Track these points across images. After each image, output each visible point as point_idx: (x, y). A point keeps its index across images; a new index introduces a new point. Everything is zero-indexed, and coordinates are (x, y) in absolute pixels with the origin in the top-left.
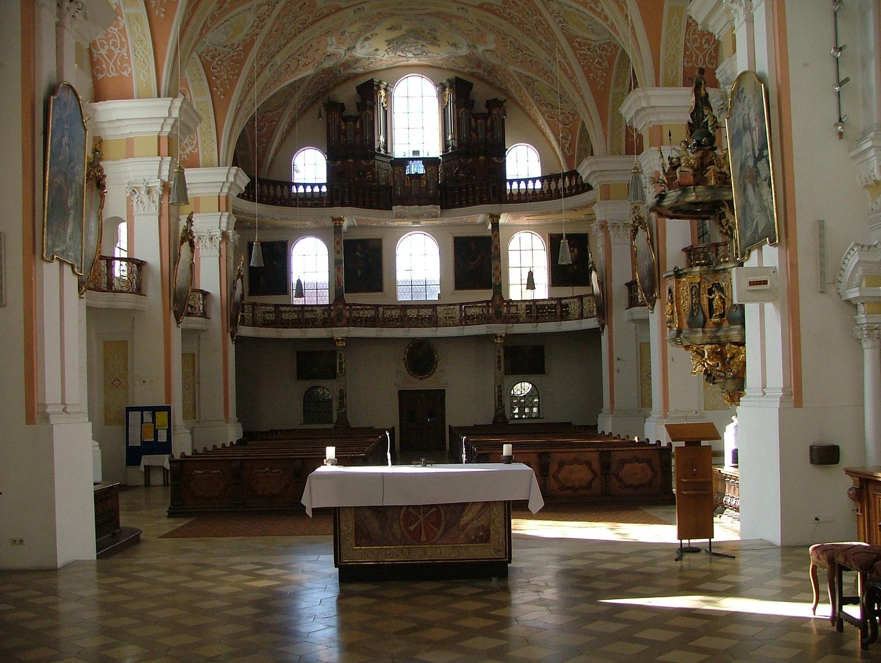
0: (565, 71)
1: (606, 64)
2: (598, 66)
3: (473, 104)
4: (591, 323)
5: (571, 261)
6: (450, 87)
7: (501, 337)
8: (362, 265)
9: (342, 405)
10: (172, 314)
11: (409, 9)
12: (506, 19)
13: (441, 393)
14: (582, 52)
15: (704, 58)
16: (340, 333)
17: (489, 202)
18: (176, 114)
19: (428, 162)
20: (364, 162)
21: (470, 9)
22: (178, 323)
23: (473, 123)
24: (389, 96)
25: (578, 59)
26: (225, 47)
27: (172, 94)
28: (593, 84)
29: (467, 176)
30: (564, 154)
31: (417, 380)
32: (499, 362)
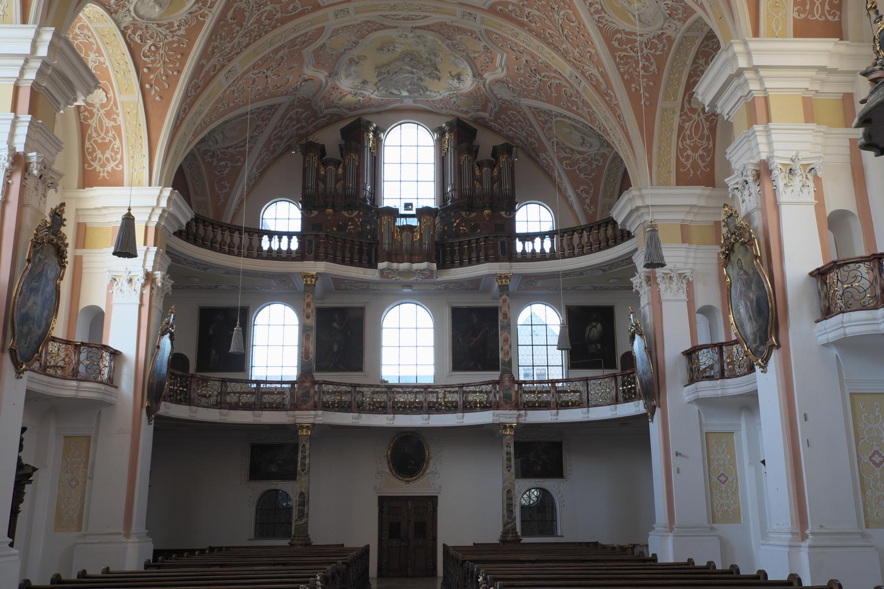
0: (597, 87)
1: (654, 68)
2: (642, 72)
3: (477, 152)
4: (633, 408)
5: (591, 338)
6: (450, 131)
7: (511, 427)
8: (340, 339)
9: (302, 514)
10: (144, 411)
11: (404, 19)
12: (522, 25)
13: (434, 500)
14: (623, 54)
15: (823, 9)
16: (307, 417)
17: (497, 260)
18: (43, 51)
19: (423, 213)
20: (345, 213)
21: (479, 15)
22: (19, 373)
23: (477, 173)
24: (378, 142)
25: (617, 64)
26: (159, 25)
27: (43, 23)
28: (634, 97)
29: (470, 220)
30: (585, 211)
31: (402, 484)
32: (509, 460)
